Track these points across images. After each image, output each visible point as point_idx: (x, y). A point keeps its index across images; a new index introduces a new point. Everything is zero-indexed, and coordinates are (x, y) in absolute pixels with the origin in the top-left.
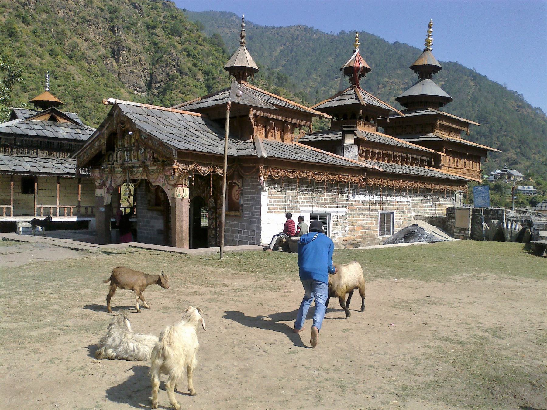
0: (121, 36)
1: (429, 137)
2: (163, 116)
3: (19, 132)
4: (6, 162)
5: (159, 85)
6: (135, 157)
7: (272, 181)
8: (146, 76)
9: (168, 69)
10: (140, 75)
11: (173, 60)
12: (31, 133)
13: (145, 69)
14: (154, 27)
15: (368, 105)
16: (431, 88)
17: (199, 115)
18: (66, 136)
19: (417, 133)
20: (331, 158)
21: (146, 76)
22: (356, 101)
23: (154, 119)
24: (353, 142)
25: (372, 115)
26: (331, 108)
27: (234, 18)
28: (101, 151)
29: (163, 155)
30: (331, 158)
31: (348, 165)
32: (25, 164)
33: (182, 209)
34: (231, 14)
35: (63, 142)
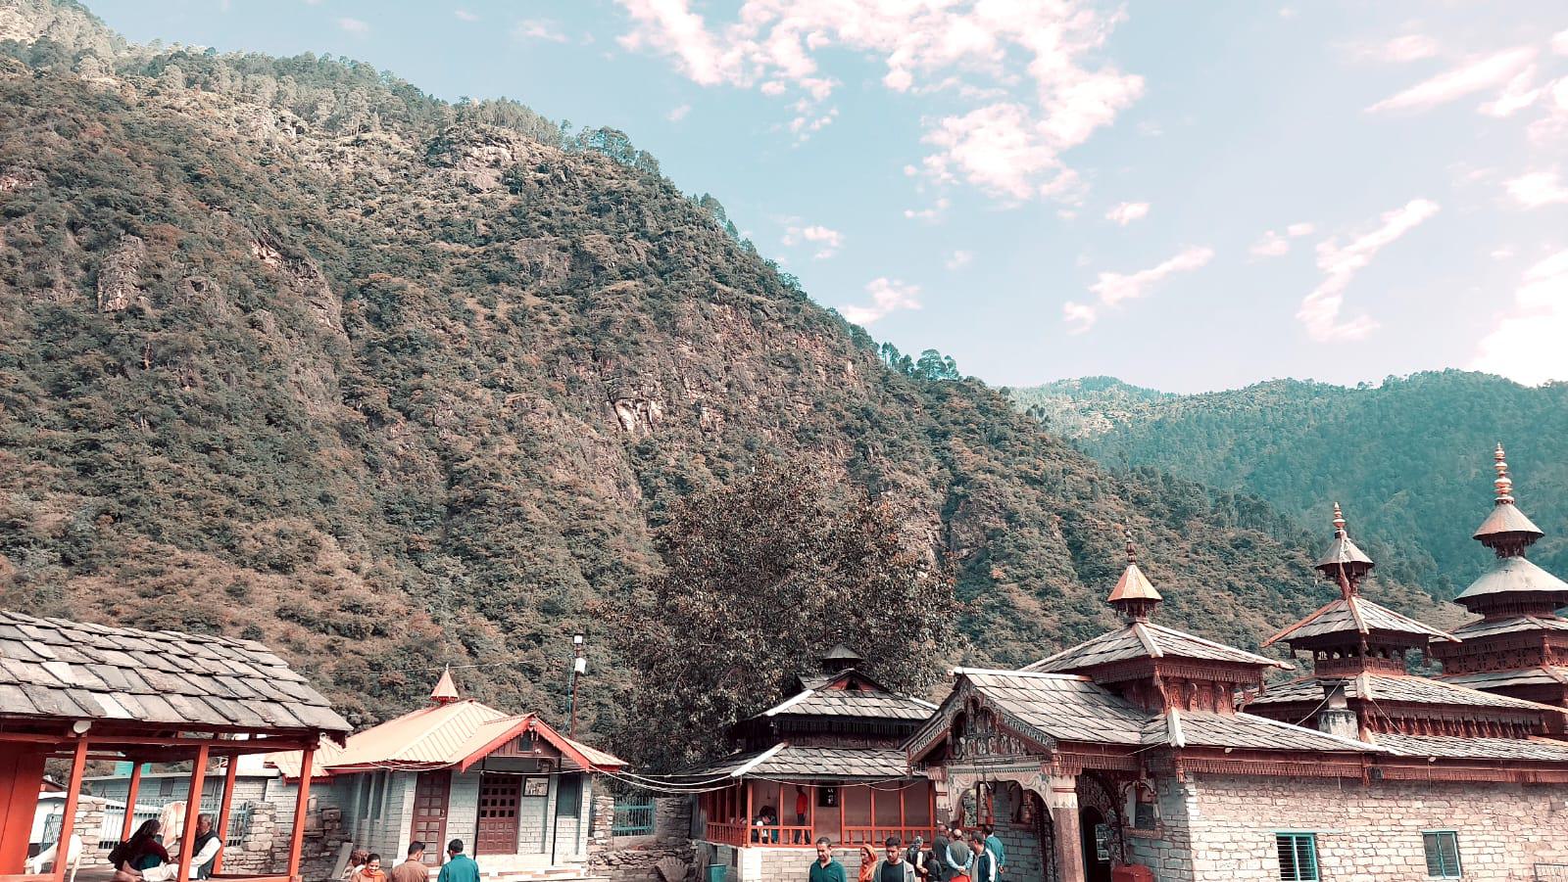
0: (881, 463)
1: (1534, 677)
2: (1029, 687)
3: (814, 711)
4: (803, 760)
5: (965, 552)
6: (993, 747)
7: (1200, 777)
8: (938, 536)
9: (982, 517)
10: (924, 536)
11: (991, 498)
12: (830, 711)
13: (933, 523)
14: (945, 435)
15: (1374, 631)
16: (1529, 576)
17: (1076, 677)
18: (875, 713)
19: (1531, 665)
20: (1300, 737)
21: (938, 536)
22: (1350, 626)
23: (1016, 693)
24: (1345, 705)
25: (1388, 648)
26: (1307, 638)
27: (1114, 388)
28: (945, 740)
29: (1038, 748)
30: (1300, 737)
31: (1332, 747)
32: (825, 761)
33: (1069, 824)
34: (1107, 382)
35: (872, 723)
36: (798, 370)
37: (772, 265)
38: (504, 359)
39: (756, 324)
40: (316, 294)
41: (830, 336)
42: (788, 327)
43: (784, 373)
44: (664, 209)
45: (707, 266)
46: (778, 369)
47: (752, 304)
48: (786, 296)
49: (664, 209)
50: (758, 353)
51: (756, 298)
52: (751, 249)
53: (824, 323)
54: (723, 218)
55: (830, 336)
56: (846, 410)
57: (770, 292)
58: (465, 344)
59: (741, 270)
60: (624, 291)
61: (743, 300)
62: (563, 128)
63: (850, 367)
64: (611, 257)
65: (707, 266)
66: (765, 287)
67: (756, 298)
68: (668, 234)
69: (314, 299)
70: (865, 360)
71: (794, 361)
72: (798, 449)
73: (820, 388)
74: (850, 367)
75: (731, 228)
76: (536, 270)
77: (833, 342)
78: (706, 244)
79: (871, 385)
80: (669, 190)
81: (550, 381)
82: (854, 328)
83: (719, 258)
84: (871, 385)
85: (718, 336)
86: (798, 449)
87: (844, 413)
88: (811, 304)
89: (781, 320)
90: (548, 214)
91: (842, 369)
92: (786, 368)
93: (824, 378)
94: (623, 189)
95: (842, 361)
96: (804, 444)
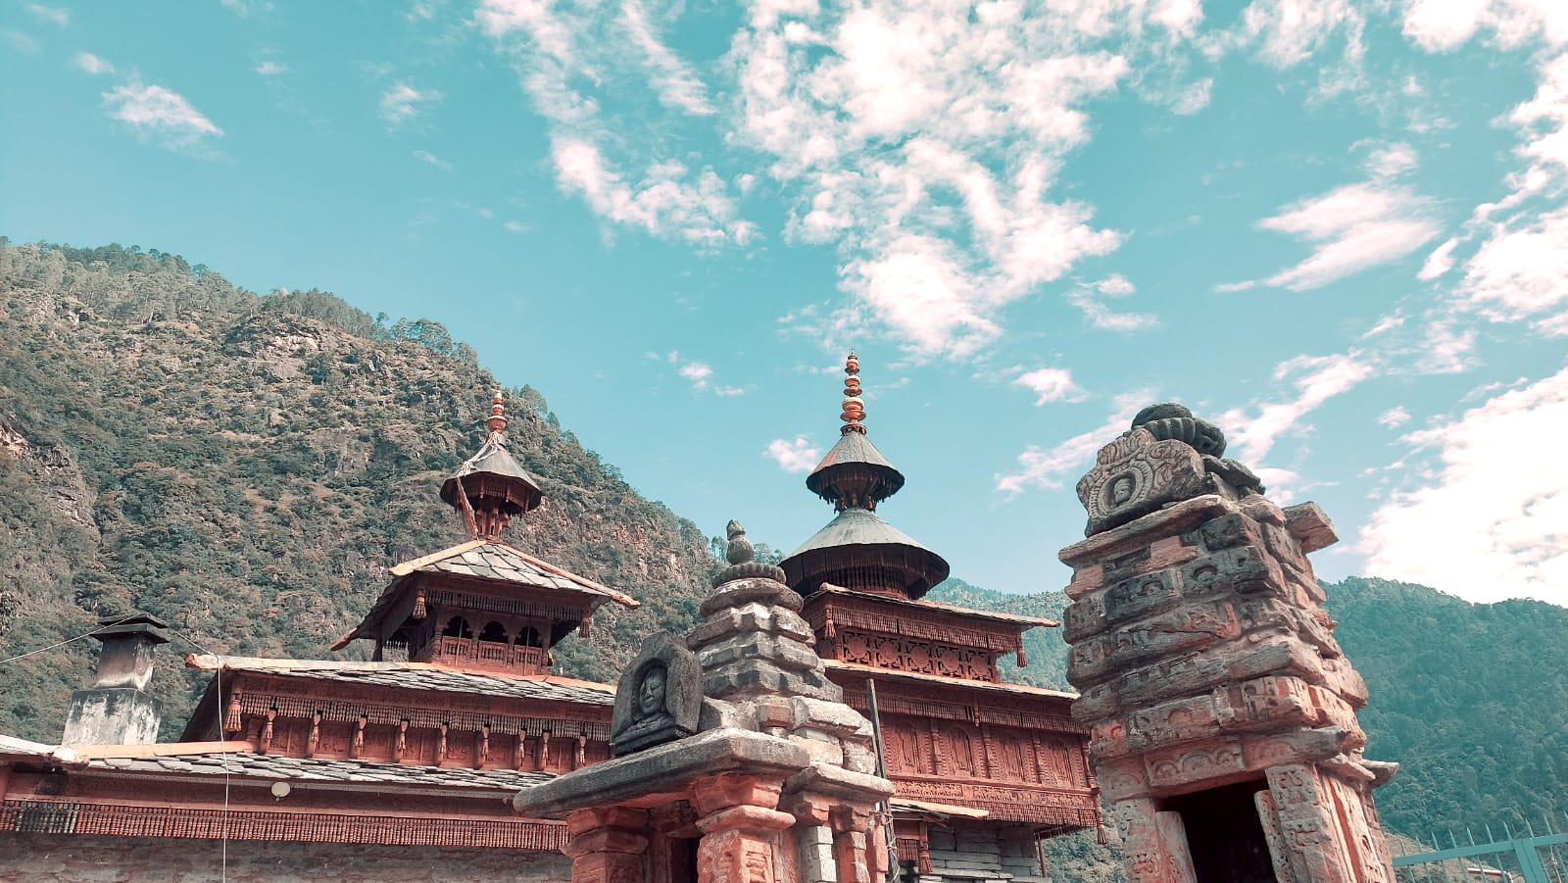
36: (616, 563)
37: (593, 457)
38: (282, 554)
39: (573, 515)
40: (65, 484)
41: (653, 528)
42: (608, 519)
43: (603, 567)
44: (479, 399)
45: (521, 456)
46: (595, 563)
47: (570, 495)
48: (606, 487)
49: (479, 399)
50: (573, 545)
51: (573, 489)
52: (574, 441)
53: (642, 515)
54: (545, 410)
55: (653, 528)
56: (669, 604)
57: (589, 483)
58: (237, 538)
59: (560, 460)
60: (427, 481)
61: (559, 490)
62: (379, 320)
63: (673, 559)
64: (417, 446)
65: (521, 456)
66: (585, 478)
67: (573, 489)
68: (481, 423)
69: (62, 489)
70: (691, 554)
71: (613, 554)
72: (614, 647)
73: (640, 581)
74: (673, 559)
75: (553, 419)
76: (331, 460)
77: (655, 534)
78: (522, 434)
79: (696, 580)
80: (485, 381)
81: (334, 578)
82: (682, 521)
83: (536, 448)
84: (696, 580)
85: (529, 528)
86: (614, 647)
87: (666, 607)
88: (634, 495)
89: (600, 511)
90: (351, 404)
91: (665, 561)
92: (604, 561)
93: (645, 572)
94: (436, 379)
95: (664, 553)
96: (621, 642)
